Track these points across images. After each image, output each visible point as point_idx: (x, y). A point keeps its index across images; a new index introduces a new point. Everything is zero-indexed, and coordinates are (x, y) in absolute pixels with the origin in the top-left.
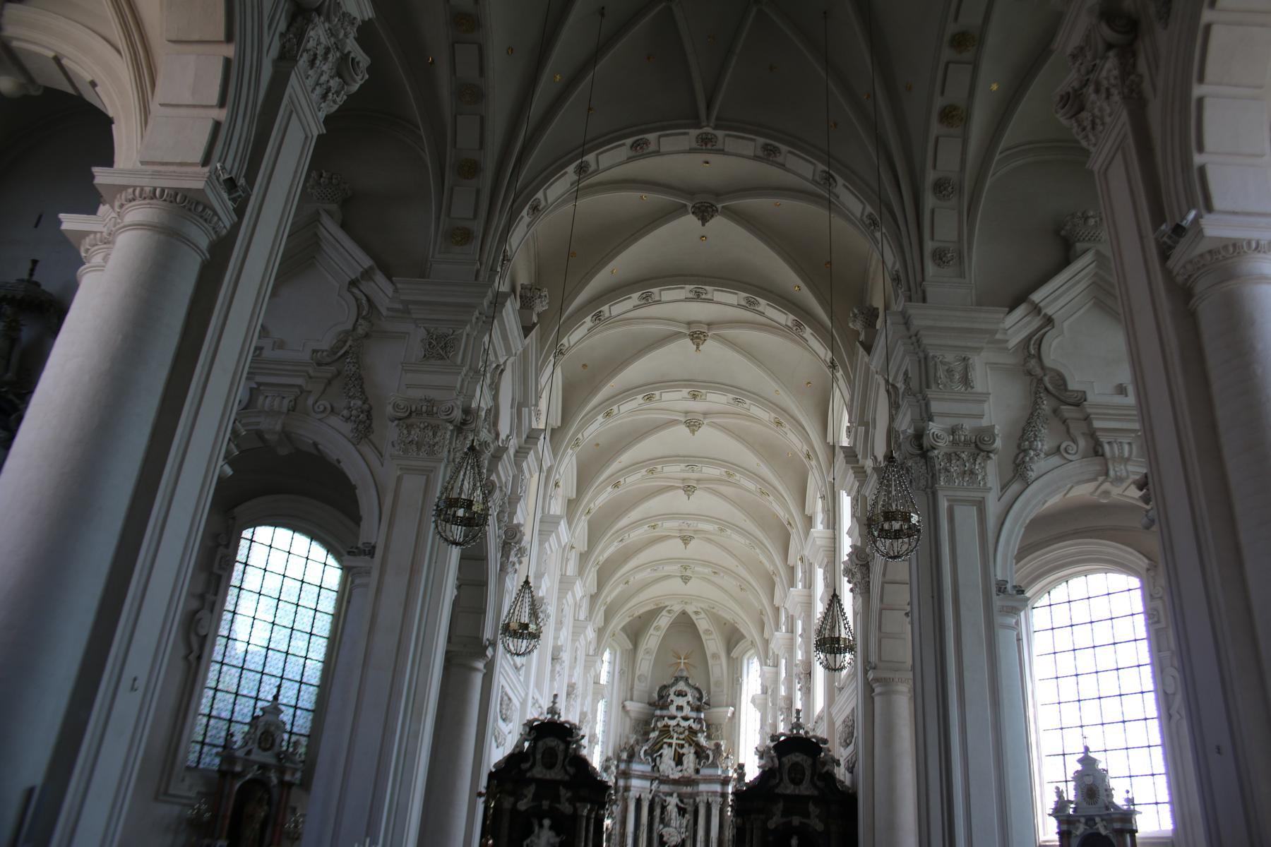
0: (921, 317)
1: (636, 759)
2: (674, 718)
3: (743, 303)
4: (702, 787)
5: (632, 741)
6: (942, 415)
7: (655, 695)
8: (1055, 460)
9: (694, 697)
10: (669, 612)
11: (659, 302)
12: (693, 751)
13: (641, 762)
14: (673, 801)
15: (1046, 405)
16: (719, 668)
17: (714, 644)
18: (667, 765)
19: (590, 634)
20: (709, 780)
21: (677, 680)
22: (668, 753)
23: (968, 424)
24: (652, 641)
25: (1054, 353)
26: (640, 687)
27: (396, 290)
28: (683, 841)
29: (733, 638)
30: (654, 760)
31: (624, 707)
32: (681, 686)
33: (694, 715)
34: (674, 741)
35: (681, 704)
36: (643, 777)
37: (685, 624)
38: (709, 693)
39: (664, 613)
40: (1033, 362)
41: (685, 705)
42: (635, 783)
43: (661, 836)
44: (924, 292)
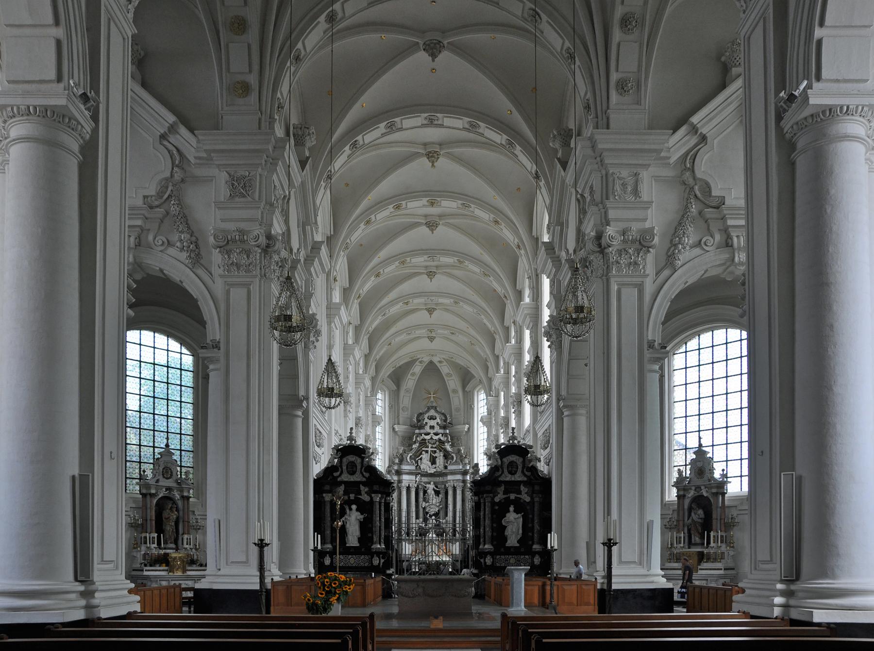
0: (604, 141)
1: (404, 462)
3: (467, 126)
4: (450, 477)
6: (617, 220)
8: (697, 251)
9: (441, 420)
10: (421, 362)
11: (401, 129)
13: (408, 464)
14: (431, 487)
15: (694, 209)
16: (457, 400)
17: (453, 383)
18: (425, 465)
19: (368, 383)
20: (453, 473)
21: (429, 409)
22: (425, 457)
23: (635, 227)
24: (410, 382)
25: (702, 169)
26: (404, 415)
27: (198, 141)
29: (466, 378)
30: (417, 462)
31: (394, 429)
33: (442, 431)
34: (429, 449)
35: (432, 426)
36: (410, 473)
37: (431, 369)
38: (451, 416)
39: (417, 363)
40: (688, 174)
41: (436, 425)
42: (405, 477)
44: (608, 119)
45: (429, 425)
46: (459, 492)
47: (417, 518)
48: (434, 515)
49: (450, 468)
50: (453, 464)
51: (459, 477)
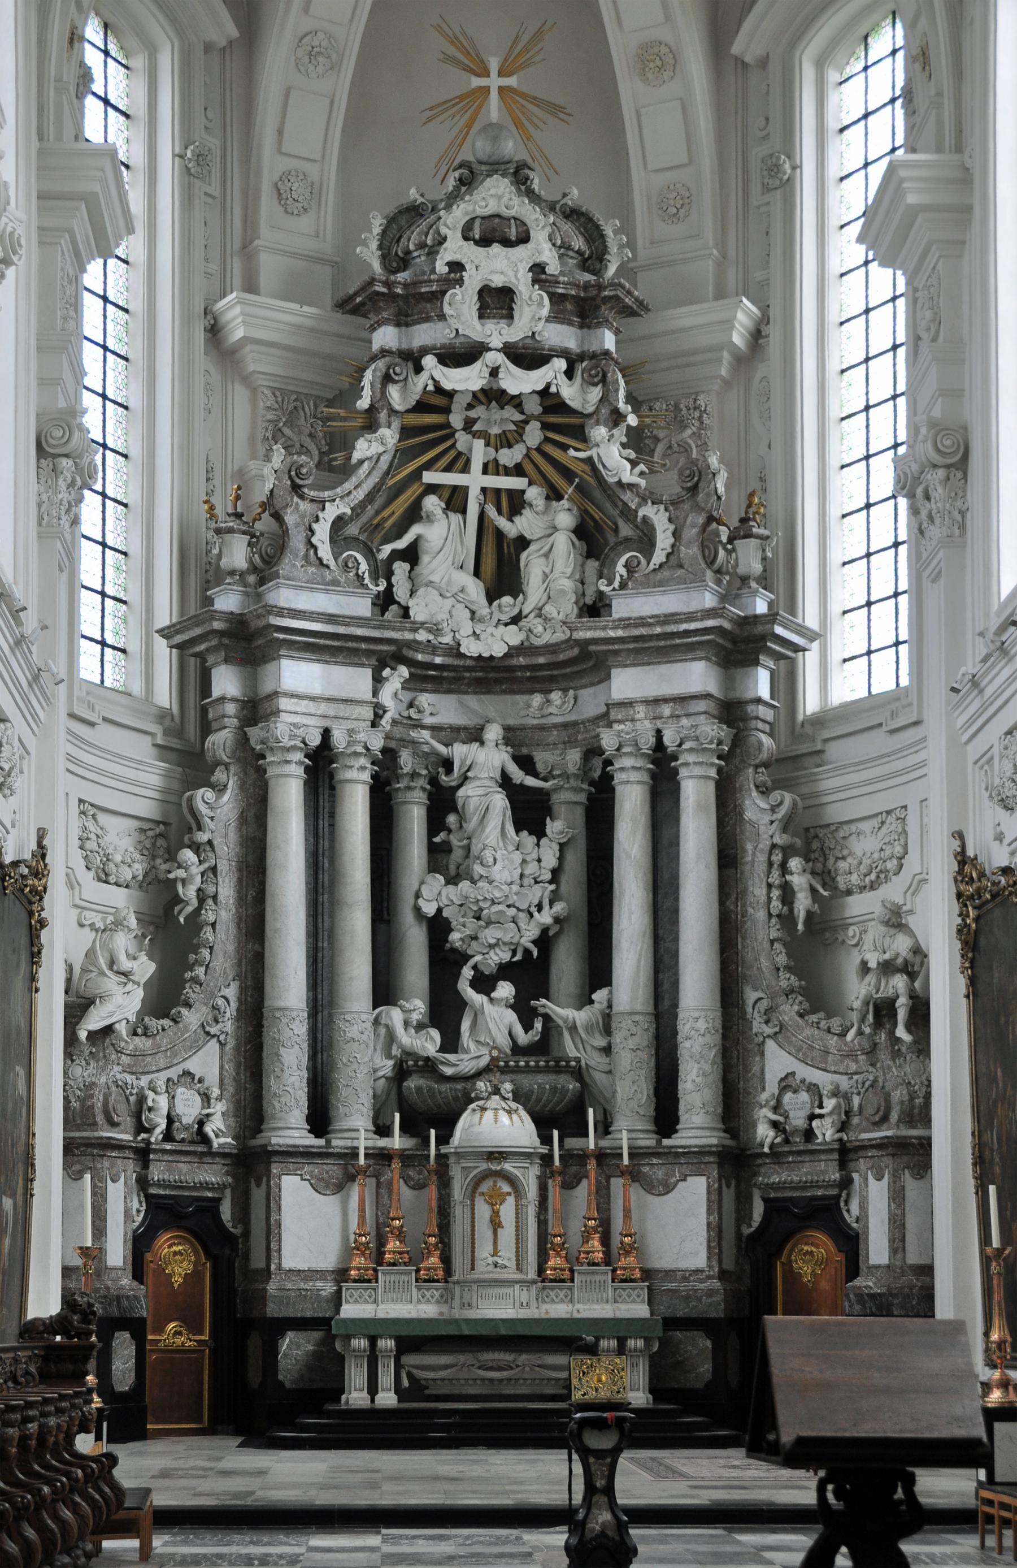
1: (291, 564)
2: (461, 355)
4: (627, 683)
5: (267, 476)
7: (371, 256)
9: (564, 248)
12: (565, 518)
14: (488, 759)
16: (669, 123)
18: (446, 597)
20: (657, 645)
21: (469, 179)
22: (445, 540)
26: (287, 237)
28: (545, 941)
30: (384, 571)
31: (214, 330)
32: (495, 196)
33: (563, 336)
34: (475, 481)
35: (502, 271)
36: (331, 646)
42: (297, 675)
43: (438, 927)
45: (473, 281)
46: (695, 793)
47: (385, 991)
48: (505, 971)
49: (626, 606)
50: (656, 581)
51: (697, 676)
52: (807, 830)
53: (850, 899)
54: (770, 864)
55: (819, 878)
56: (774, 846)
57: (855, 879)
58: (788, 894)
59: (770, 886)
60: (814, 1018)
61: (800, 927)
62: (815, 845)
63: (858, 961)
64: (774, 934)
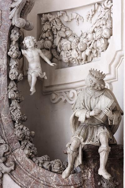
52: (40, 15)
53: (70, 69)
54: (10, 41)
55: (48, 53)
56: (12, 27)
57: (74, 54)
58: (23, 66)
59: (9, 58)
60: (40, 159)
61: (32, 89)
62: (46, 27)
63: (72, 116)
64: (11, 95)
